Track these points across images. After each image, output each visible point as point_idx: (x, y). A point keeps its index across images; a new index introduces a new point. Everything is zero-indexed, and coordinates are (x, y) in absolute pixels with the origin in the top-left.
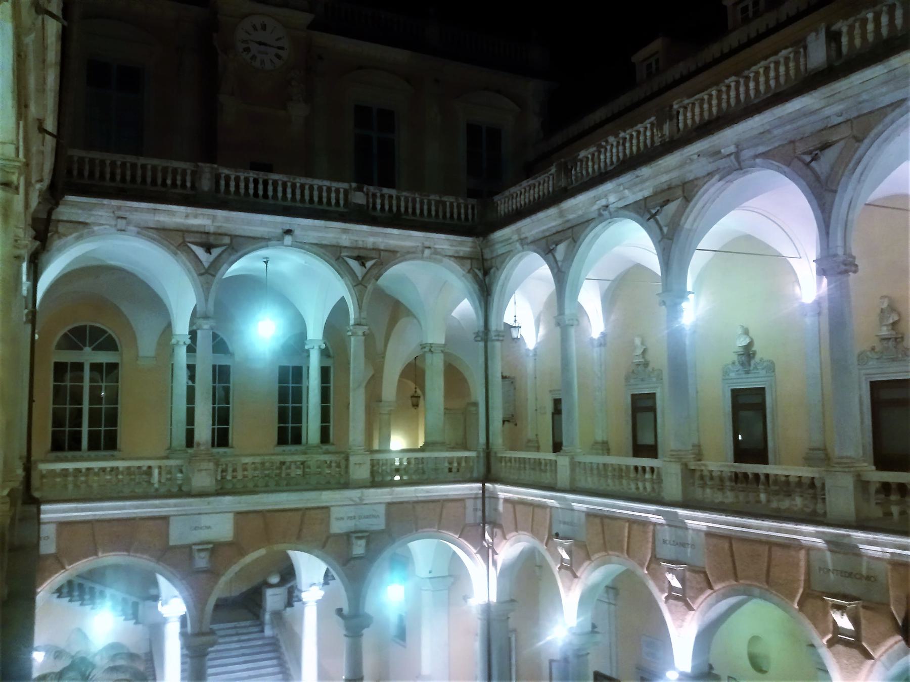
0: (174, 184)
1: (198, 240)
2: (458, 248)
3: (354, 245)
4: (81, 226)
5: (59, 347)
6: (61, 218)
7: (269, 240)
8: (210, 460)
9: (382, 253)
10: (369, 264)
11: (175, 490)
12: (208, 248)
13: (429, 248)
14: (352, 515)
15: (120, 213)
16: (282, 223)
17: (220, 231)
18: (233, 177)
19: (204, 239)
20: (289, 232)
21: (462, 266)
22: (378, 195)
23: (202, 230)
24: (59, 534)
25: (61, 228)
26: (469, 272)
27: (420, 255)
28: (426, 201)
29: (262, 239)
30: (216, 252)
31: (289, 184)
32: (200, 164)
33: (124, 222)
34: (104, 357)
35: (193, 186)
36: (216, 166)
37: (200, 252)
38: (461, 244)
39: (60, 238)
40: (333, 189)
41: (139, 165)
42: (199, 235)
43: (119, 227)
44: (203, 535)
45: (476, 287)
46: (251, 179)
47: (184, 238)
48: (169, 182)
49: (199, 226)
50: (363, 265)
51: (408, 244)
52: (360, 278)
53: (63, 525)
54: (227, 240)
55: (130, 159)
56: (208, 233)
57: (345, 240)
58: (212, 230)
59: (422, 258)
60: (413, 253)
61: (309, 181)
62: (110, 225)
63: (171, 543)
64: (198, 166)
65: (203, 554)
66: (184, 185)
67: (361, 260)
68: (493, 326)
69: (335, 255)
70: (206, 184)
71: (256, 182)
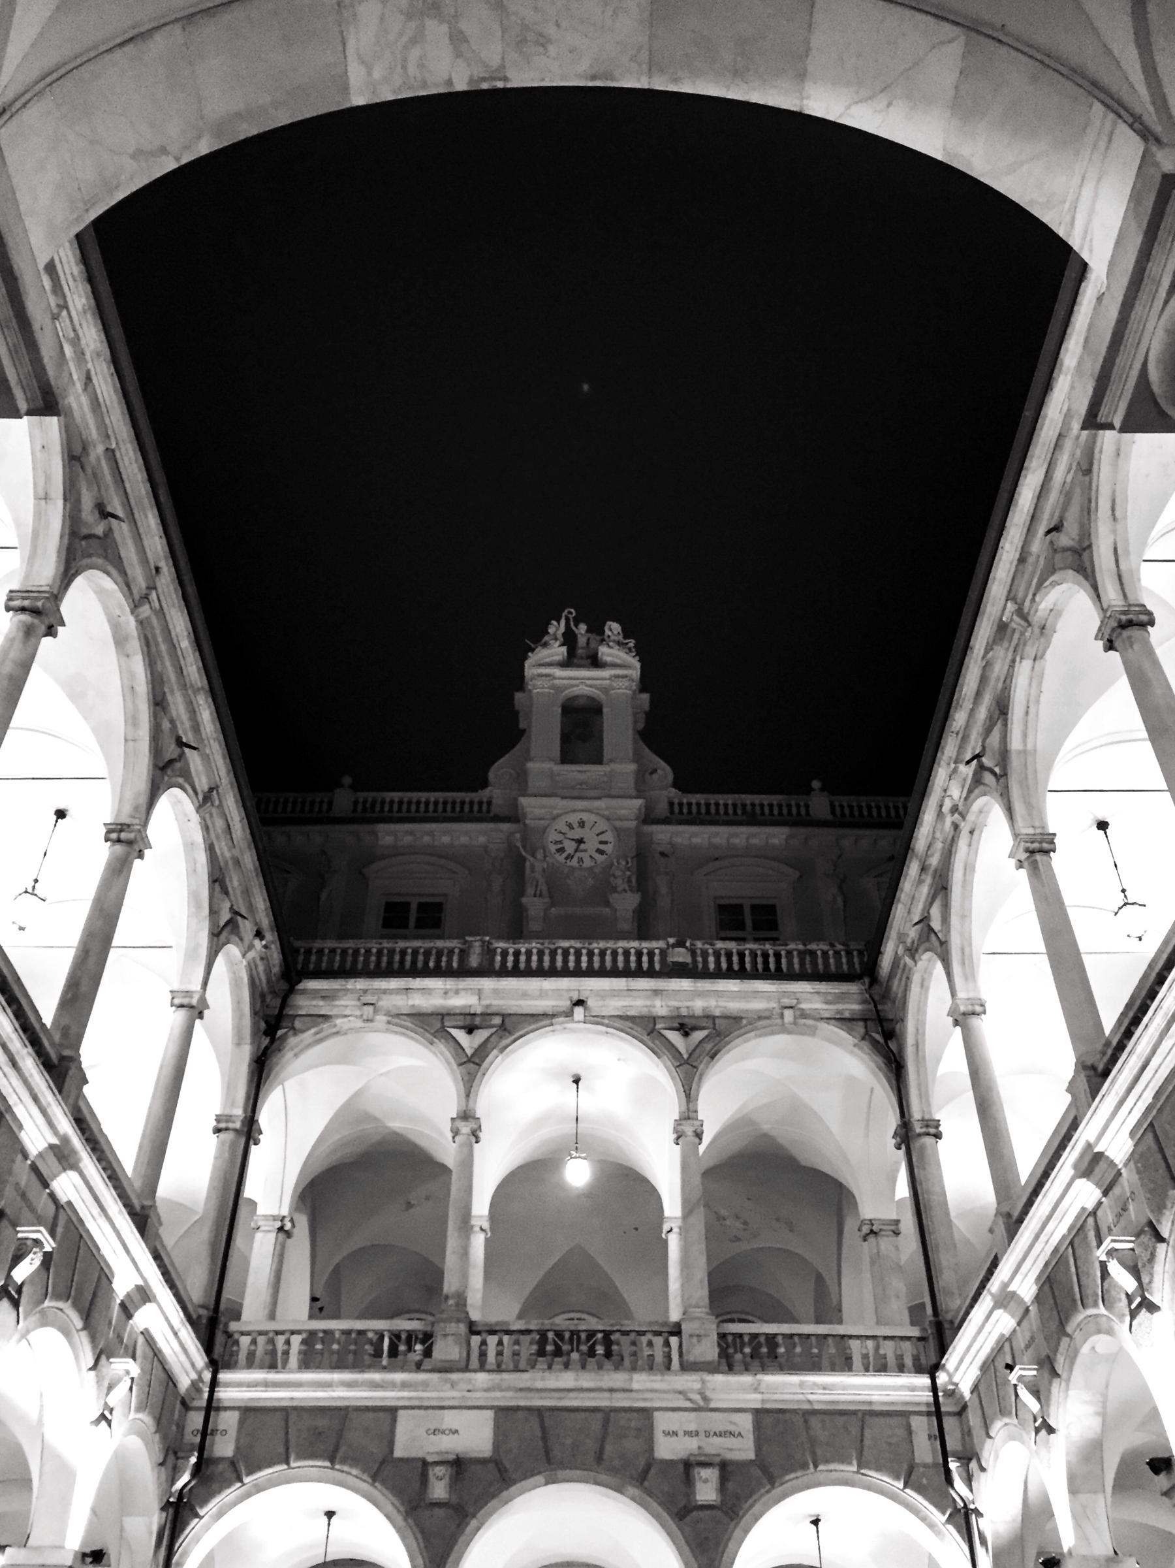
1: (460, 1024)
2: (841, 1007)
3: (675, 1014)
4: (320, 1020)
6: (300, 1013)
7: (553, 1016)
9: (717, 1021)
10: (698, 1035)
12: (470, 1031)
14: (692, 1427)
16: (569, 990)
17: (489, 1011)
18: (511, 951)
19: (468, 1021)
20: (580, 1003)
21: (850, 1031)
22: (710, 951)
23: (467, 1011)
24: (242, 1422)
25: (298, 1024)
26: (863, 1039)
27: (779, 1021)
28: (783, 953)
29: (545, 1015)
30: (481, 1036)
31: (584, 951)
32: (468, 938)
33: (371, 1008)
36: (487, 938)
37: (460, 1035)
38: (841, 998)
39: (295, 1035)
40: (645, 951)
41: (398, 950)
42: (459, 1017)
43: (365, 1017)
44: (449, 1445)
45: (880, 1060)
46: (535, 951)
47: (442, 1023)
49: (465, 1007)
51: (758, 1005)
52: (685, 1056)
53: (248, 1412)
54: (497, 1021)
55: (387, 944)
56: (474, 1014)
57: (660, 1008)
58: (479, 1011)
59: (784, 1030)
61: (610, 944)
62: (356, 1017)
63: (398, 1454)
64: (465, 942)
65: (440, 1470)
67: (685, 1029)
68: (916, 1113)
69: (646, 1029)
70: (474, 961)
71: (541, 953)
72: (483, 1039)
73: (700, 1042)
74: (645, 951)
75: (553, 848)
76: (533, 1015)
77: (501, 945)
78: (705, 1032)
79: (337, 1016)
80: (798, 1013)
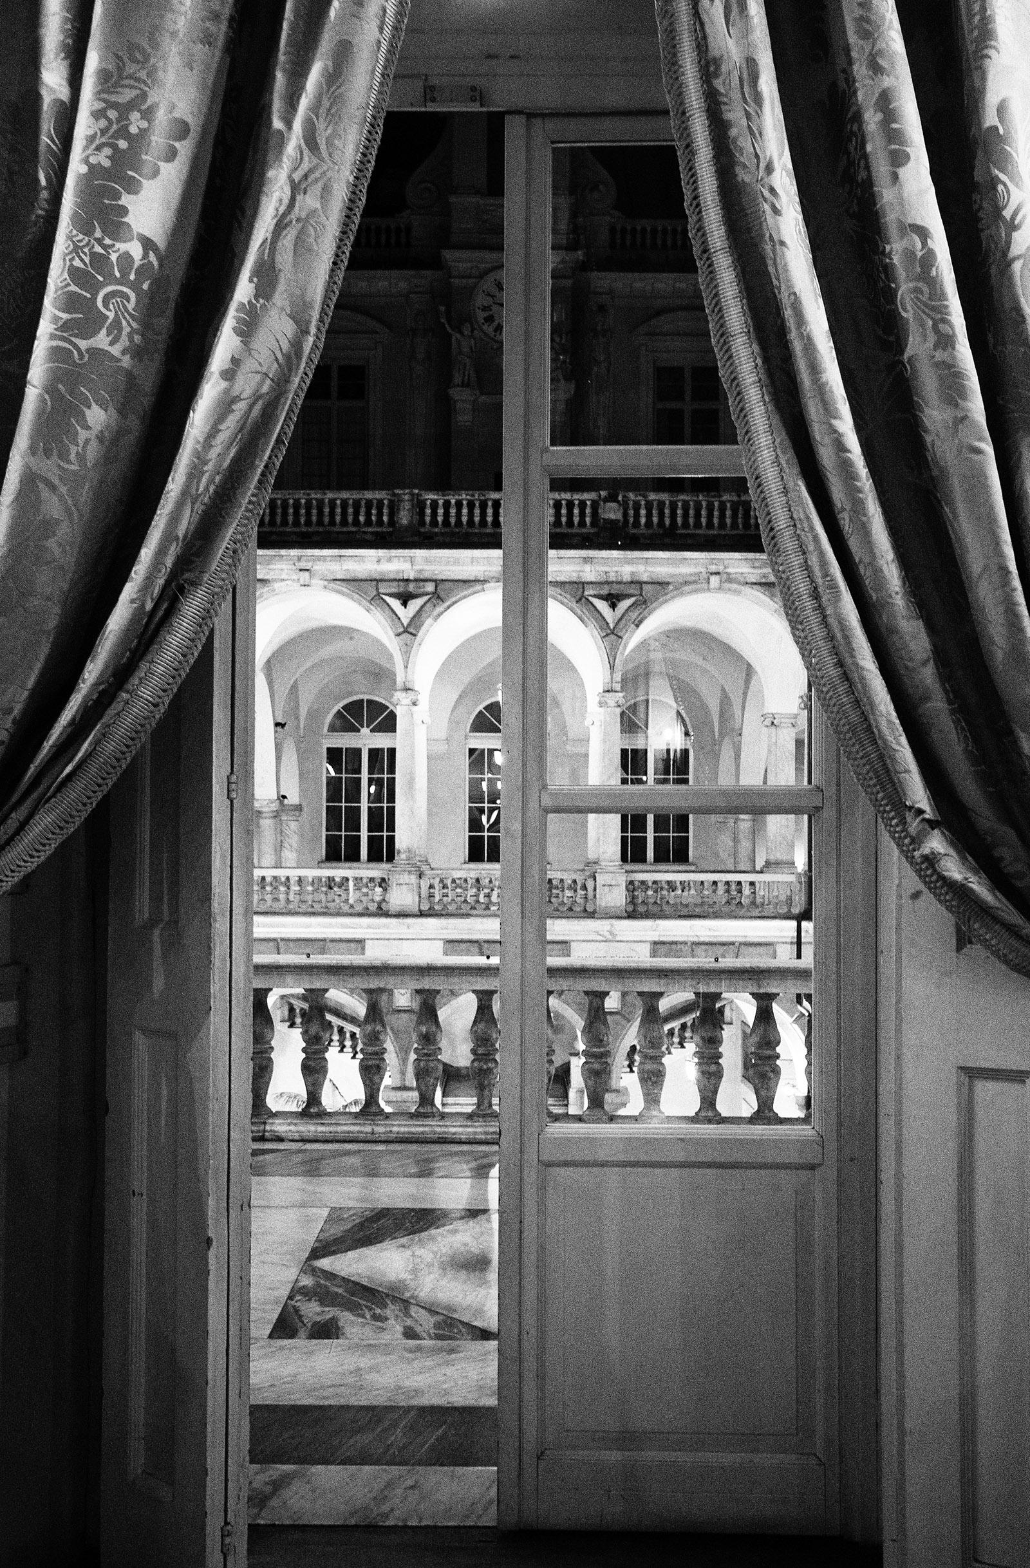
0: (368, 522)
3: (603, 578)
5: (333, 728)
7: (485, 581)
8: (410, 872)
9: (645, 587)
10: (624, 605)
11: (373, 907)
12: (405, 599)
13: (718, 573)
15: (303, 565)
18: (441, 502)
22: (643, 503)
27: (705, 586)
29: (476, 581)
30: (415, 605)
32: (397, 491)
33: (307, 574)
34: (381, 741)
35: (392, 522)
37: (395, 604)
42: (394, 584)
47: (377, 589)
48: (362, 519)
50: (613, 606)
51: (685, 570)
54: (430, 587)
55: (315, 495)
56: (407, 580)
57: (590, 573)
60: (695, 582)
64: (394, 495)
66: (380, 522)
67: (613, 600)
70: (404, 518)
71: (471, 505)
72: (417, 608)
73: (627, 610)
74: (577, 502)
75: (481, 315)
76: (465, 582)
77: (430, 496)
78: (633, 599)
79: (275, 580)
80: (725, 577)
